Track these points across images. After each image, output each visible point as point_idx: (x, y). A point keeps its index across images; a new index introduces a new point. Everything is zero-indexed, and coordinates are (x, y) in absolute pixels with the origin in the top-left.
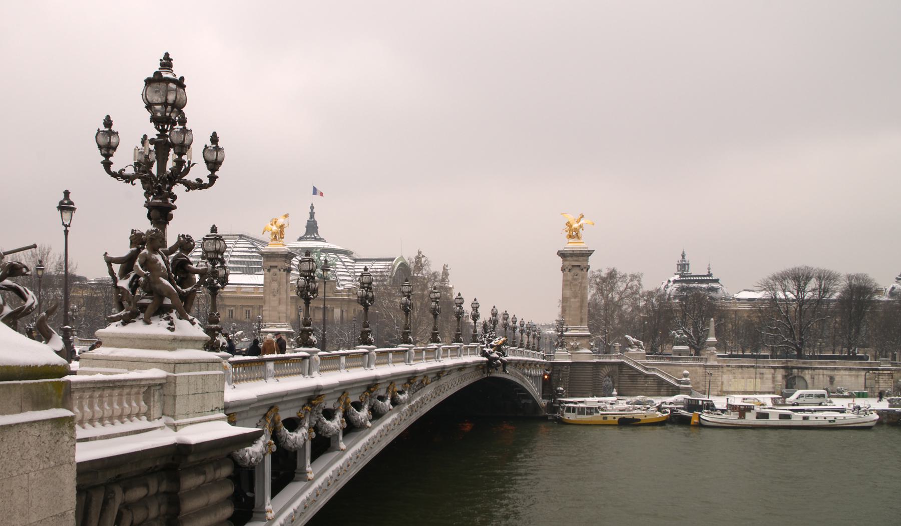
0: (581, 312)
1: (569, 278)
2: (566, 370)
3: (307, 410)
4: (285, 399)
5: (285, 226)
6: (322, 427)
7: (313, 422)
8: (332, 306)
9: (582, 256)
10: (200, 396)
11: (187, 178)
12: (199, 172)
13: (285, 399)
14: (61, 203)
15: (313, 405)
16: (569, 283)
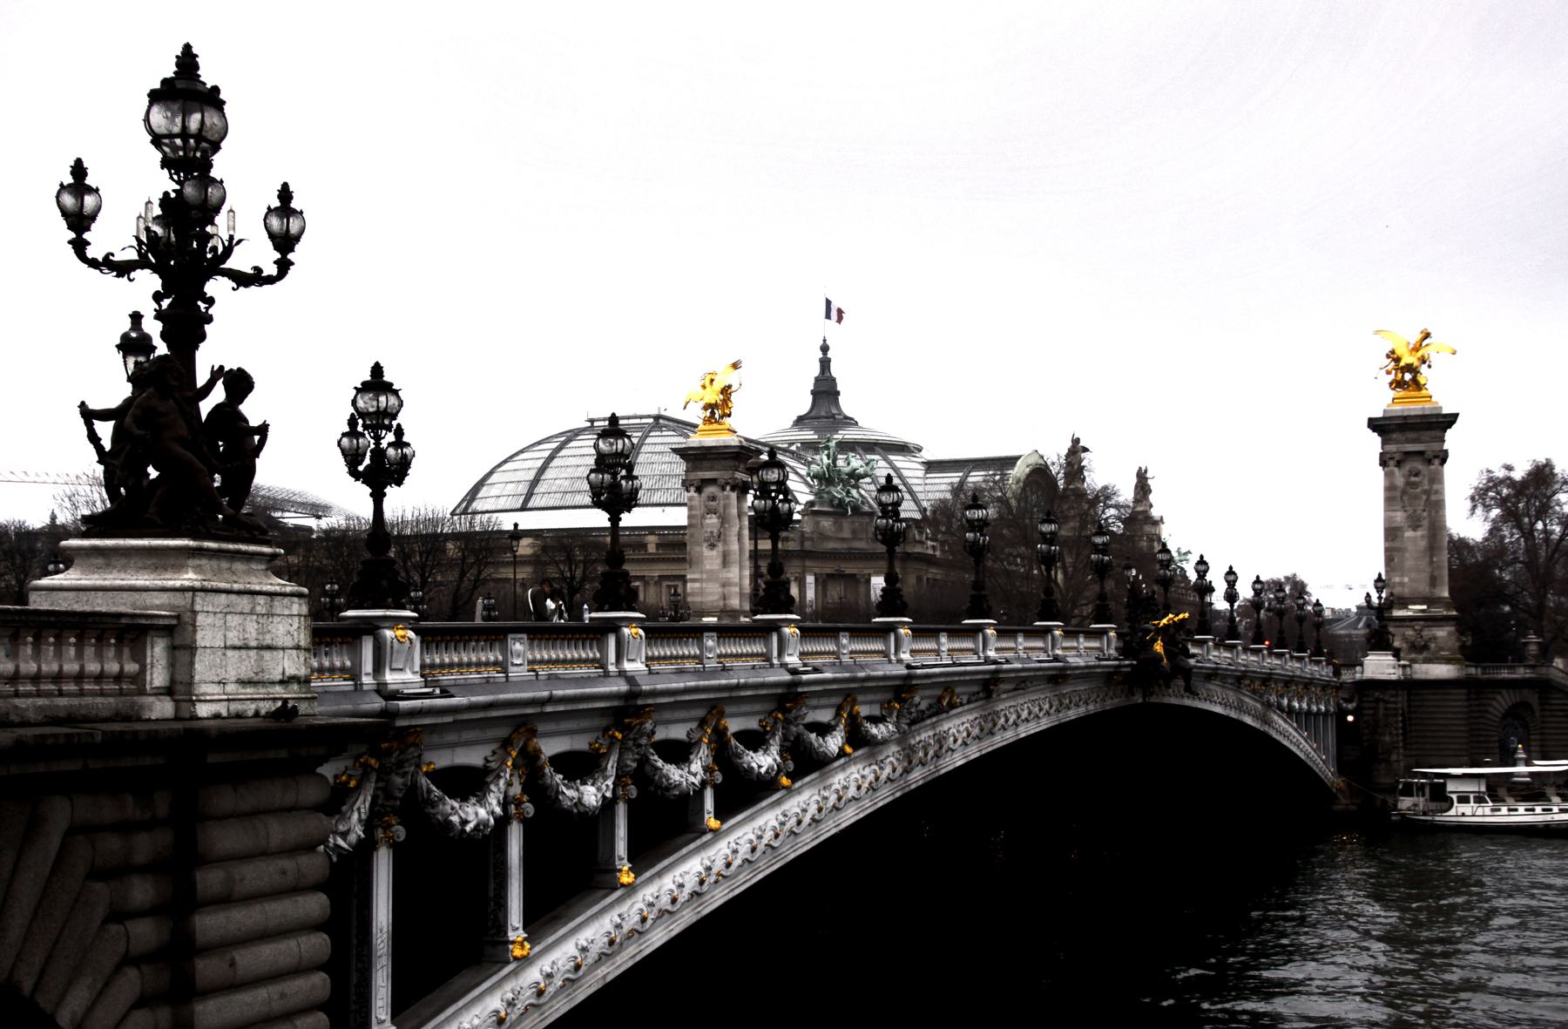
0: (1431, 562)
1: (1400, 481)
2: (1392, 699)
3: (613, 737)
4: (549, 709)
5: (733, 389)
6: (654, 775)
7: (629, 762)
8: (866, 571)
10: (253, 653)
11: (230, 264)
12: (255, 253)
13: (549, 709)
14: (125, 337)
15: (626, 729)
16: (1398, 494)
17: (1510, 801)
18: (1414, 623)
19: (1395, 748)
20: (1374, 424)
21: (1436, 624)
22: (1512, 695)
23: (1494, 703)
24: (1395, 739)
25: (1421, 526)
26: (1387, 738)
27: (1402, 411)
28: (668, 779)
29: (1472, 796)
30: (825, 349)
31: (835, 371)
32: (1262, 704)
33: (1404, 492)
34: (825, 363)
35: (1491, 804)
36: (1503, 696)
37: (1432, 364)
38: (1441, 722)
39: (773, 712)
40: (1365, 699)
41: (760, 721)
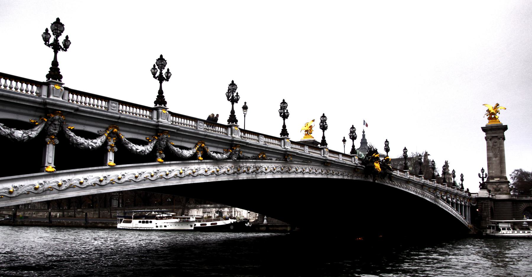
0: (501, 167)
1: (491, 145)
5: (313, 126)
6: (70, 138)
9: (499, 130)
16: (490, 148)
17: (518, 229)
18: (496, 184)
19: (488, 216)
20: (484, 129)
21: (502, 184)
22: (526, 204)
23: (521, 207)
24: (487, 214)
25: (498, 157)
26: (485, 214)
27: (491, 125)
28: (77, 141)
29: (506, 228)
30: (364, 132)
31: (366, 137)
32: (435, 196)
33: (492, 147)
34: (364, 136)
35: (512, 230)
36: (524, 205)
37: (500, 113)
38: (504, 211)
39: (153, 136)
40: (479, 203)
41: (146, 138)
